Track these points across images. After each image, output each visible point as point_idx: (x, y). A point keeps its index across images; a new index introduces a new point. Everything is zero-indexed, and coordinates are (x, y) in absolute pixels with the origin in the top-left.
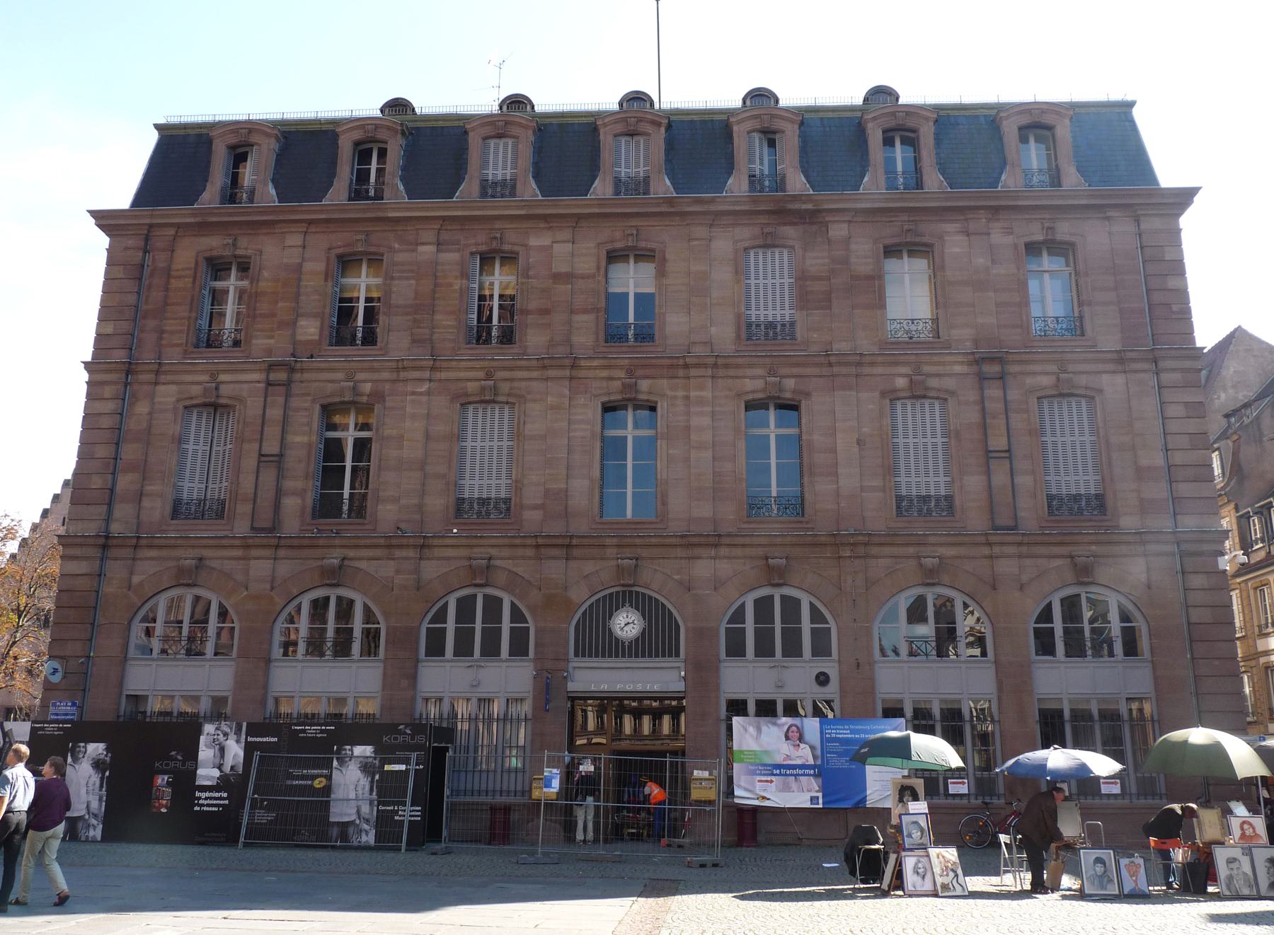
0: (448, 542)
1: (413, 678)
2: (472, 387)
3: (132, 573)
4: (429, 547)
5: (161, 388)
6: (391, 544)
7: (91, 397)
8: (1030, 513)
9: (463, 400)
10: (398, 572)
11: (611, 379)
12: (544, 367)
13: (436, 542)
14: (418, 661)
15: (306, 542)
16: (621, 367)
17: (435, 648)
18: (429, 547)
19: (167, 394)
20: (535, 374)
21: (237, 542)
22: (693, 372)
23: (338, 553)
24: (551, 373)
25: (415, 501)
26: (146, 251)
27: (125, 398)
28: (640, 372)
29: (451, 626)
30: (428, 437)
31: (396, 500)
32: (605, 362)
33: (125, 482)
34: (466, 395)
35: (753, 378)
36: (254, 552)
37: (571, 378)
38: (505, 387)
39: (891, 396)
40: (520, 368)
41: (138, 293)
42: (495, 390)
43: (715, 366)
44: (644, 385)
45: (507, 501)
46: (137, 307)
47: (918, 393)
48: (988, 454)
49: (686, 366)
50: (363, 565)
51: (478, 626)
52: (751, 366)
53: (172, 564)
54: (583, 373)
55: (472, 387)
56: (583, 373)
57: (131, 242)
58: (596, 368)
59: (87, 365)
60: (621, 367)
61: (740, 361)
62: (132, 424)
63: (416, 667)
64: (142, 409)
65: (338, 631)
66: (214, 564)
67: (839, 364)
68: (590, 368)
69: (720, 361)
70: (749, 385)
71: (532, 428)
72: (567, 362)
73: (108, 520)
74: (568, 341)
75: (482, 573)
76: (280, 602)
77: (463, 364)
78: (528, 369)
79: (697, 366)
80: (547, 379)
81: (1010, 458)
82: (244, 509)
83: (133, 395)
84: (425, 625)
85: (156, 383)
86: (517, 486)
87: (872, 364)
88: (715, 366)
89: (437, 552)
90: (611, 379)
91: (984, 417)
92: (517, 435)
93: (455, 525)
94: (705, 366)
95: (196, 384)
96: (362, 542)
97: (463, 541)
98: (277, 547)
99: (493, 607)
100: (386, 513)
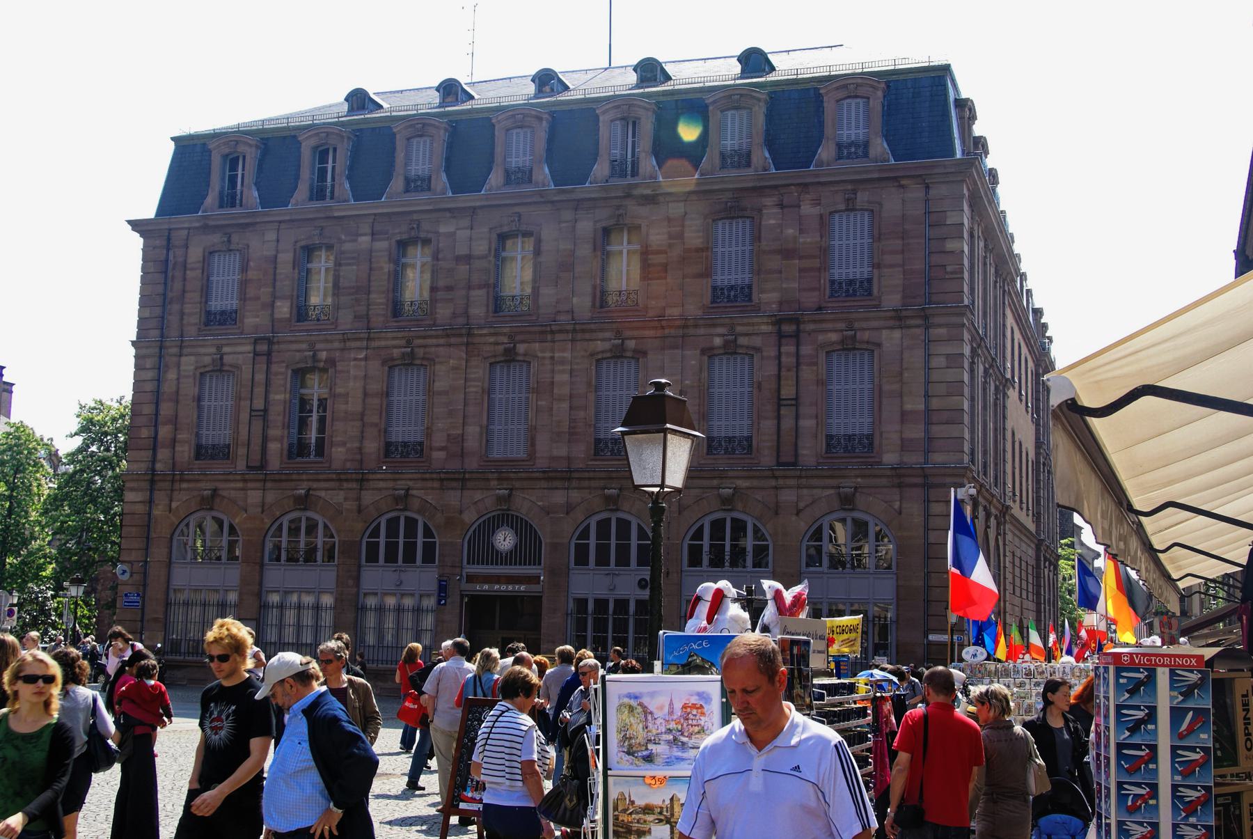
0: (379, 476)
1: (358, 579)
2: (396, 352)
3: (171, 501)
4: (368, 480)
5: (184, 359)
6: (341, 478)
7: (139, 367)
8: (809, 451)
9: (391, 364)
10: (346, 499)
11: (497, 344)
12: (448, 336)
13: (371, 477)
14: (360, 566)
15: (283, 477)
16: (505, 334)
17: (372, 557)
18: (368, 480)
19: (188, 364)
20: (442, 341)
21: (239, 477)
22: (558, 337)
23: (305, 485)
24: (453, 340)
25: (357, 445)
26: (168, 250)
27: (160, 368)
28: (518, 338)
29: (382, 540)
30: (365, 394)
31: (344, 444)
32: (492, 331)
33: (164, 432)
34: (392, 359)
35: (602, 340)
36: (250, 485)
37: (467, 344)
38: (420, 352)
39: (709, 352)
40: (431, 337)
41: (165, 284)
42: (412, 355)
43: (574, 331)
44: (521, 348)
45: (421, 444)
46: (164, 294)
47: (731, 348)
48: (780, 402)
49: (552, 332)
50: (322, 494)
51: (401, 540)
52: (602, 330)
53: (196, 493)
54: (477, 340)
55: (396, 352)
56: (477, 340)
57: (158, 242)
58: (485, 335)
59: (133, 343)
60: (505, 334)
61: (593, 326)
62: (168, 388)
63: (359, 571)
64: (172, 375)
65: (307, 544)
66: (224, 493)
67: (670, 327)
68: (481, 335)
69: (578, 327)
70: (600, 346)
71: (439, 385)
72: (464, 331)
73: (154, 461)
74: (466, 314)
75: (403, 500)
76: (268, 522)
77: (390, 335)
78: (437, 337)
79: (560, 331)
80: (450, 345)
81: (797, 406)
82: (242, 451)
83: (166, 366)
84: (365, 540)
85: (181, 356)
86: (429, 433)
87: (696, 326)
88: (574, 331)
89: (372, 484)
90: (497, 344)
91: (780, 370)
92: (430, 392)
93: (384, 463)
94: (567, 332)
95: (207, 353)
96: (321, 477)
97: (390, 476)
98: (265, 481)
99: (411, 524)
100: (338, 454)
